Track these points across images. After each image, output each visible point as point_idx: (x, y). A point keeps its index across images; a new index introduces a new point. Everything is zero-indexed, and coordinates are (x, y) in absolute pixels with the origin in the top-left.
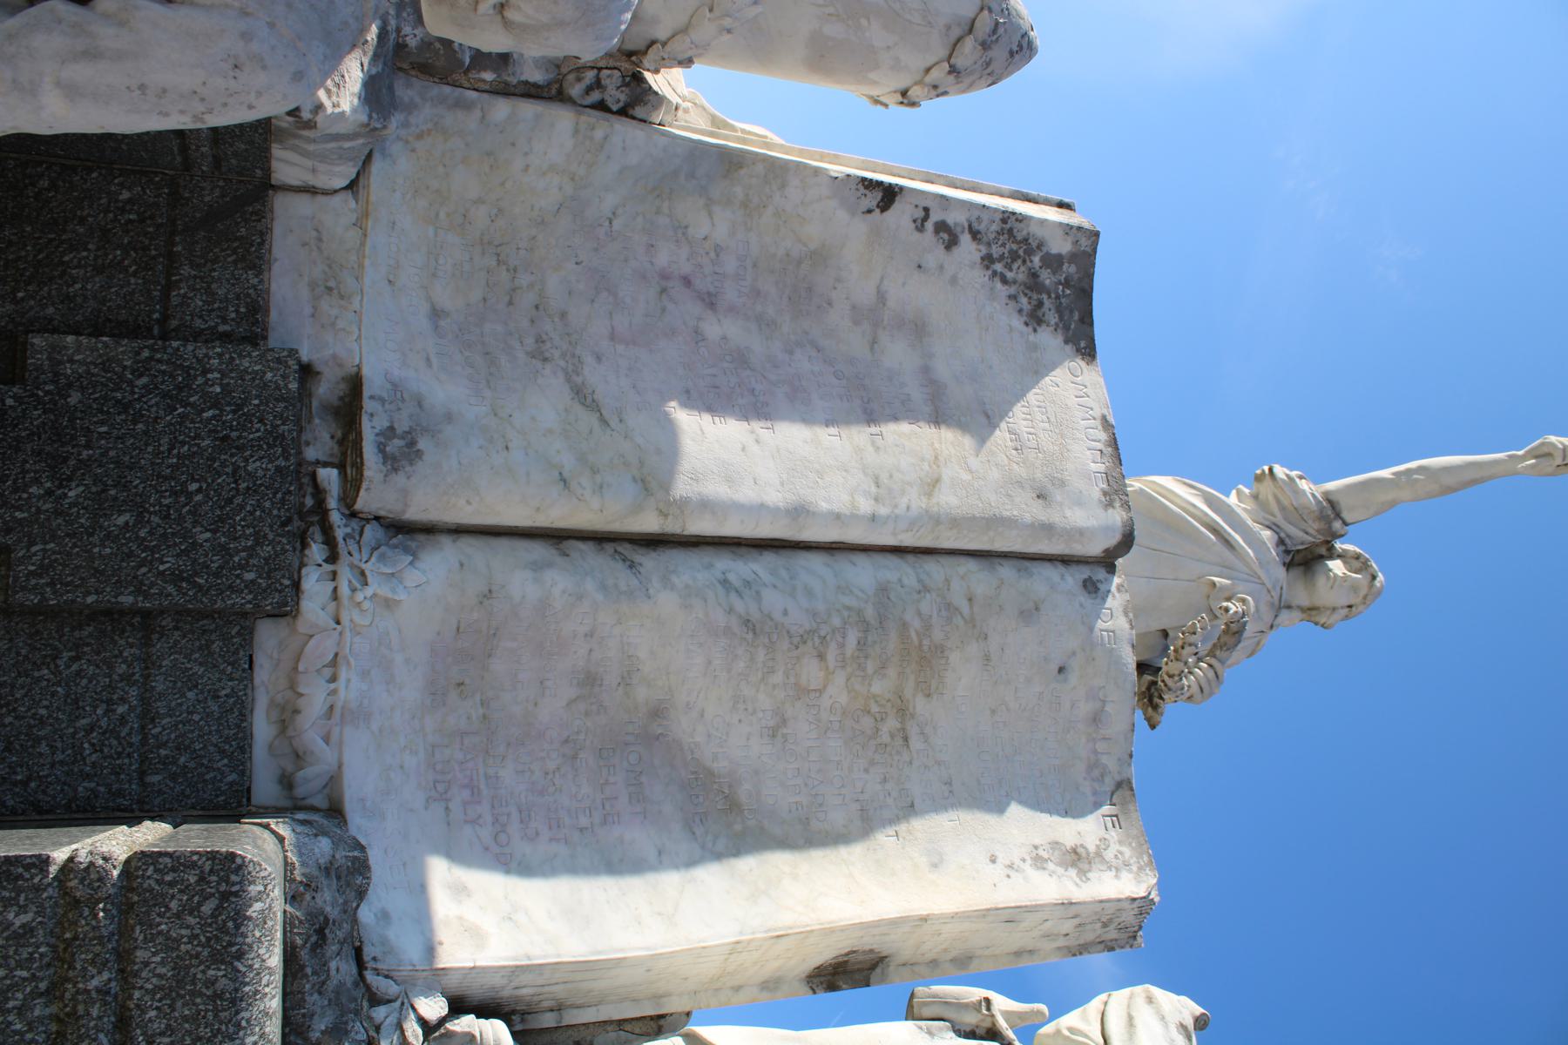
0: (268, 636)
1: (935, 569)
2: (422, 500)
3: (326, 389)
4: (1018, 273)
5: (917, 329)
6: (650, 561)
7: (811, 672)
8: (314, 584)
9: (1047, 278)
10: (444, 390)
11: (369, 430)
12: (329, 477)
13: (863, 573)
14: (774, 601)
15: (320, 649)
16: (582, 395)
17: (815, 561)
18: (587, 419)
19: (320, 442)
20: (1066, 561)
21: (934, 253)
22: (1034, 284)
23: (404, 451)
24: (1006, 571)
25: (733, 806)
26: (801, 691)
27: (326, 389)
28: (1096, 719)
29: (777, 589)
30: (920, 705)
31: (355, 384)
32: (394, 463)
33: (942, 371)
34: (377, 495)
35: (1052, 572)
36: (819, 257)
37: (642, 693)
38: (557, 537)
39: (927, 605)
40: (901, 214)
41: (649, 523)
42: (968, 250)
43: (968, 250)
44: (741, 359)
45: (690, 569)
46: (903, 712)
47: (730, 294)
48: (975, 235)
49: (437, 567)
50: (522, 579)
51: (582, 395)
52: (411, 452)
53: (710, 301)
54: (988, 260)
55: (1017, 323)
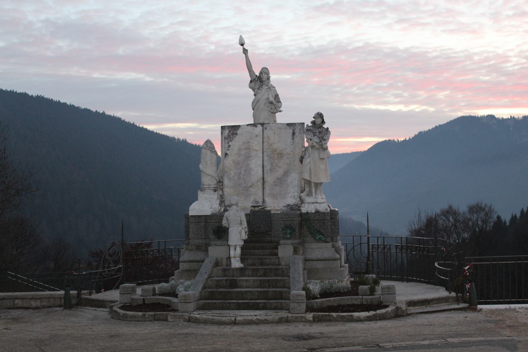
0: (272, 212)
1: (265, 149)
2: (260, 201)
3: (253, 208)
4: (232, 136)
5: (240, 150)
6: (265, 180)
7: (275, 164)
8: (268, 209)
9: (232, 132)
10: (252, 199)
11: (256, 205)
12: (260, 208)
13: (265, 158)
14: (268, 168)
15: (273, 208)
16: (251, 186)
17: (264, 163)
18: (253, 186)
19: (257, 209)
20: (263, 131)
21: (231, 148)
22: (232, 134)
23: (257, 202)
24: (265, 140)
25: (286, 172)
26: (277, 165)
27: (253, 208)
28: (280, 128)
29: (268, 167)
30: (278, 152)
31: (252, 206)
32: (258, 203)
33: (244, 147)
34: (261, 204)
35: (264, 134)
36: (234, 162)
37: (277, 181)
38: (263, 188)
39: (268, 151)
40: (228, 152)
41: (262, 181)
42: (230, 143)
43: (230, 143)
44: (245, 170)
45: (266, 176)
46: (278, 154)
47: (239, 171)
48: (229, 143)
49: (267, 199)
50: (267, 191)
51: (251, 186)
52: (257, 201)
53: (240, 173)
54: (231, 141)
55: (237, 137)
